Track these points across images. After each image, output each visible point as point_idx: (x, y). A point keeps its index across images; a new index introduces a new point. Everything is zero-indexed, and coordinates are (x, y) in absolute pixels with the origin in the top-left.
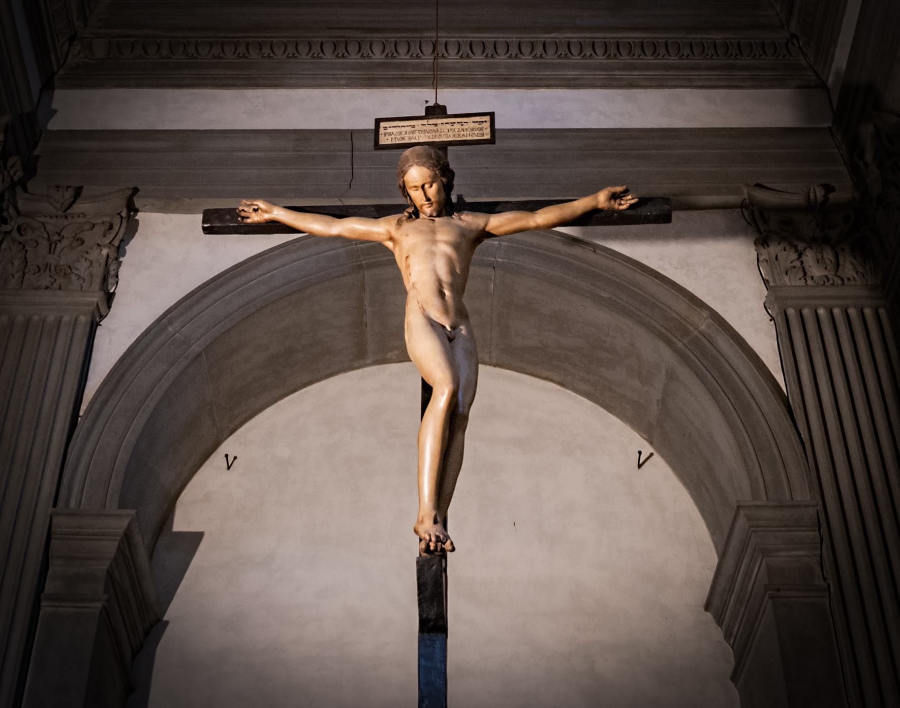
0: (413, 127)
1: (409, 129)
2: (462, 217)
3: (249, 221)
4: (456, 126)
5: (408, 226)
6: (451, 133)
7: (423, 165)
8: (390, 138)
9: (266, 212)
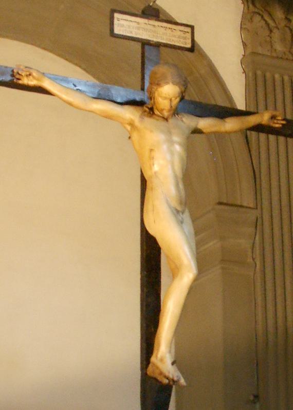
0: (138, 23)
1: (135, 25)
2: (184, 119)
3: (20, 82)
4: (169, 31)
5: (149, 121)
6: (165, 37)
7: (173, 83)
8: (122, 29)
9: (38, 80)
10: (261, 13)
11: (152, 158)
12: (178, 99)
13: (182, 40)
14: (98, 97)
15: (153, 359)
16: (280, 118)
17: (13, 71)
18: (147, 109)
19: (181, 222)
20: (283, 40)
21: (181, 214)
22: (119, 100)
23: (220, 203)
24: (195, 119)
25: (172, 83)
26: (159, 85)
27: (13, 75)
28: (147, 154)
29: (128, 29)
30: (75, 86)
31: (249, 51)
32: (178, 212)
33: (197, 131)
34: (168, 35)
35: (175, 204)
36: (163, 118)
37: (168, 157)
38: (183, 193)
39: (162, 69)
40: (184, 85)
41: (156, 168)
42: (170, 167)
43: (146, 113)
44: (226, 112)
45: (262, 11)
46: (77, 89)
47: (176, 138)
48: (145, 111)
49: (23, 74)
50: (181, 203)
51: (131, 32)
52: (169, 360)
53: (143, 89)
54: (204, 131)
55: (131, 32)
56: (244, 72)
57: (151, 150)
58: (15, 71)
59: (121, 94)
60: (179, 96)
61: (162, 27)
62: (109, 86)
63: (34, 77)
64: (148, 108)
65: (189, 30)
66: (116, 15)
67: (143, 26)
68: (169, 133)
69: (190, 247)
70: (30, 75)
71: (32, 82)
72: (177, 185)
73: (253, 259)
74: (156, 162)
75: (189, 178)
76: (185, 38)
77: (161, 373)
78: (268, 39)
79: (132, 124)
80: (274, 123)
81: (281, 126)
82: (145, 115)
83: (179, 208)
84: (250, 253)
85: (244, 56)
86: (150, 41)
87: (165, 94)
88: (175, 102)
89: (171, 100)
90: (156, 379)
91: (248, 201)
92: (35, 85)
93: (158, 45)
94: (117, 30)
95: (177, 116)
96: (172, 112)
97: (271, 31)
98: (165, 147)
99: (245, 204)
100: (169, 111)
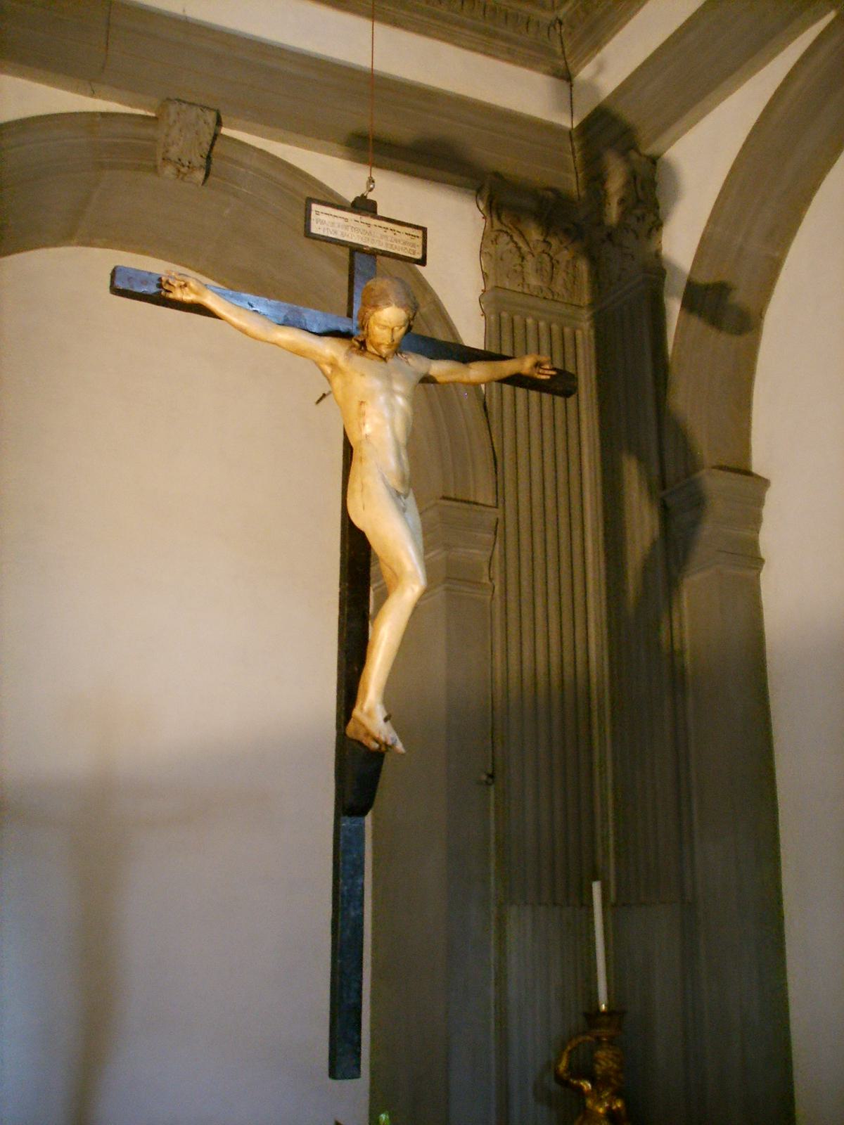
0: (346, 220)
1: (341, 221)
2: (410, 360)
3: (171, 296)
4: (389, 233)
5: (357, 359)
6: (383, 241)
7: (400, 306)
8: (322, 226)
9: (197, 293)
10: (509, 231)
11: (362, 415)
12: (403, 330)
13: (409, 248)
14: (286, 323)
15: (356, 712)
16: (548, 367)
17: (160, 279)
18: (357, 343)
19: (403, 510)
20: (539, 271)
21: (402, 498)
22: (315, 330)
23: (444, 498)
24: (425, 360)
25: (396, 304)
26: (375, 306)
27: (160, 286)
28: (355, 405)
29: (331, 228)
30: (252, 306)
31: (491, 284)
32: (398, 494)
33: (427, 380)
34: (389, 238)
35: (394, 482)
36: (381, 357)
37: (386, 414)
38: (407, 469)
39: (379, 284)
40: (413, 309)
41: (368, 429)
42: (388, 427)
43: (355, 349)
44: (467, 356)
45: (510, 229)
46: (255, 311)
47: (398, 387)
48: (354, 346)
49: (175, 285)
50: (403, 481)
51: (336, 232)
52: (380, 714)
53: (350, 315)
54: (439, 379)
55: (336, 232)
56: (484, 314)
57: (362, 403)
58: (163, 278)
59: (318, 319)
60: (404, 326)
61: (380, 227)
62: (301, 308)
63: (191, 289)
64: (358, 341)
65: (419, 233)
66: (315, 207)
67: (352, 224)
68: (389, 378)
69: (416, 546)
70: (185, 285)
71: (188, 297)
72: (399, 457)
73: (491, 579)
74: (368, 420)
75: (418, 447)
76: (414, 245)
77: (368, 734)
78: (518, 268)
79: (333, 365)
80: (539, 373)
81: (548, 377)
82: (352, 352)
83: (401, 490)
84: (486, 570)
85: (484, 291)
86: (363, 246)
87: (385, 321)
88: (399, 333)
89: (393, 329)
90: (360, 743)
91: (485, 495)
92: (192, 301)
93: (374, 253)
94: (316, 229)
95: (399, 355)
96: (393, 348)
97: (523, 258)
98: (382, 399)
99: (481, 501)
100: (390, 346)
